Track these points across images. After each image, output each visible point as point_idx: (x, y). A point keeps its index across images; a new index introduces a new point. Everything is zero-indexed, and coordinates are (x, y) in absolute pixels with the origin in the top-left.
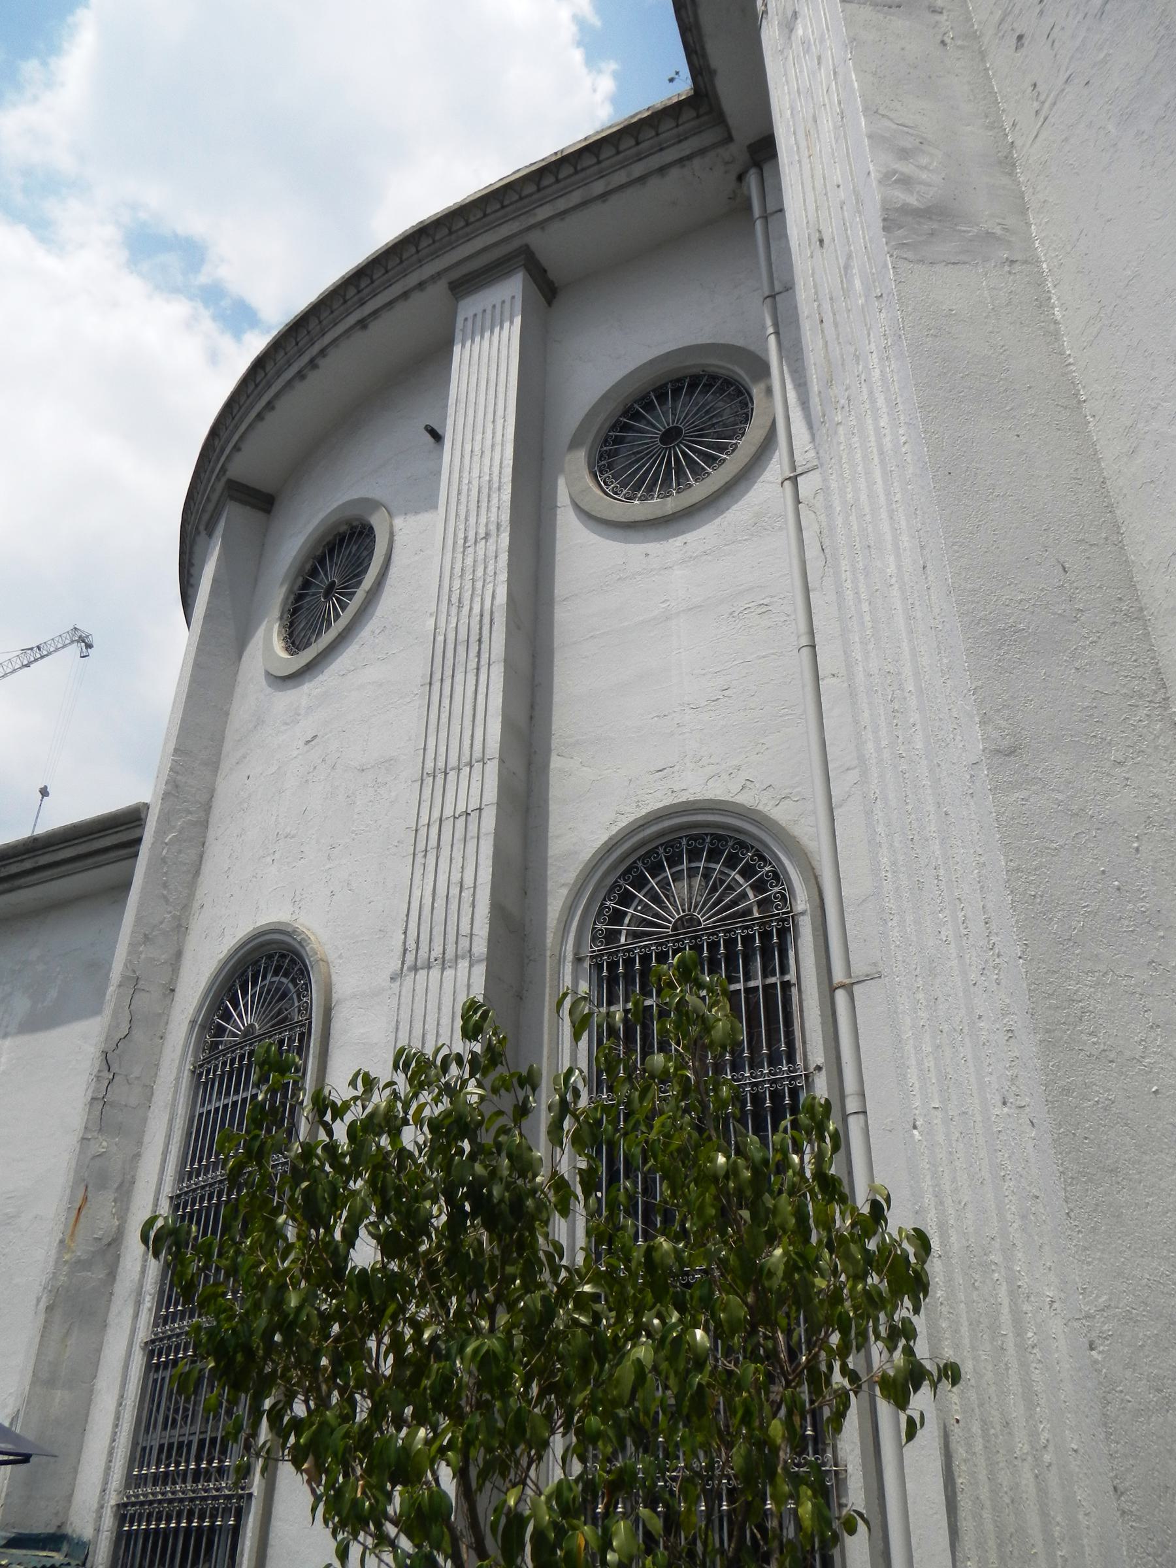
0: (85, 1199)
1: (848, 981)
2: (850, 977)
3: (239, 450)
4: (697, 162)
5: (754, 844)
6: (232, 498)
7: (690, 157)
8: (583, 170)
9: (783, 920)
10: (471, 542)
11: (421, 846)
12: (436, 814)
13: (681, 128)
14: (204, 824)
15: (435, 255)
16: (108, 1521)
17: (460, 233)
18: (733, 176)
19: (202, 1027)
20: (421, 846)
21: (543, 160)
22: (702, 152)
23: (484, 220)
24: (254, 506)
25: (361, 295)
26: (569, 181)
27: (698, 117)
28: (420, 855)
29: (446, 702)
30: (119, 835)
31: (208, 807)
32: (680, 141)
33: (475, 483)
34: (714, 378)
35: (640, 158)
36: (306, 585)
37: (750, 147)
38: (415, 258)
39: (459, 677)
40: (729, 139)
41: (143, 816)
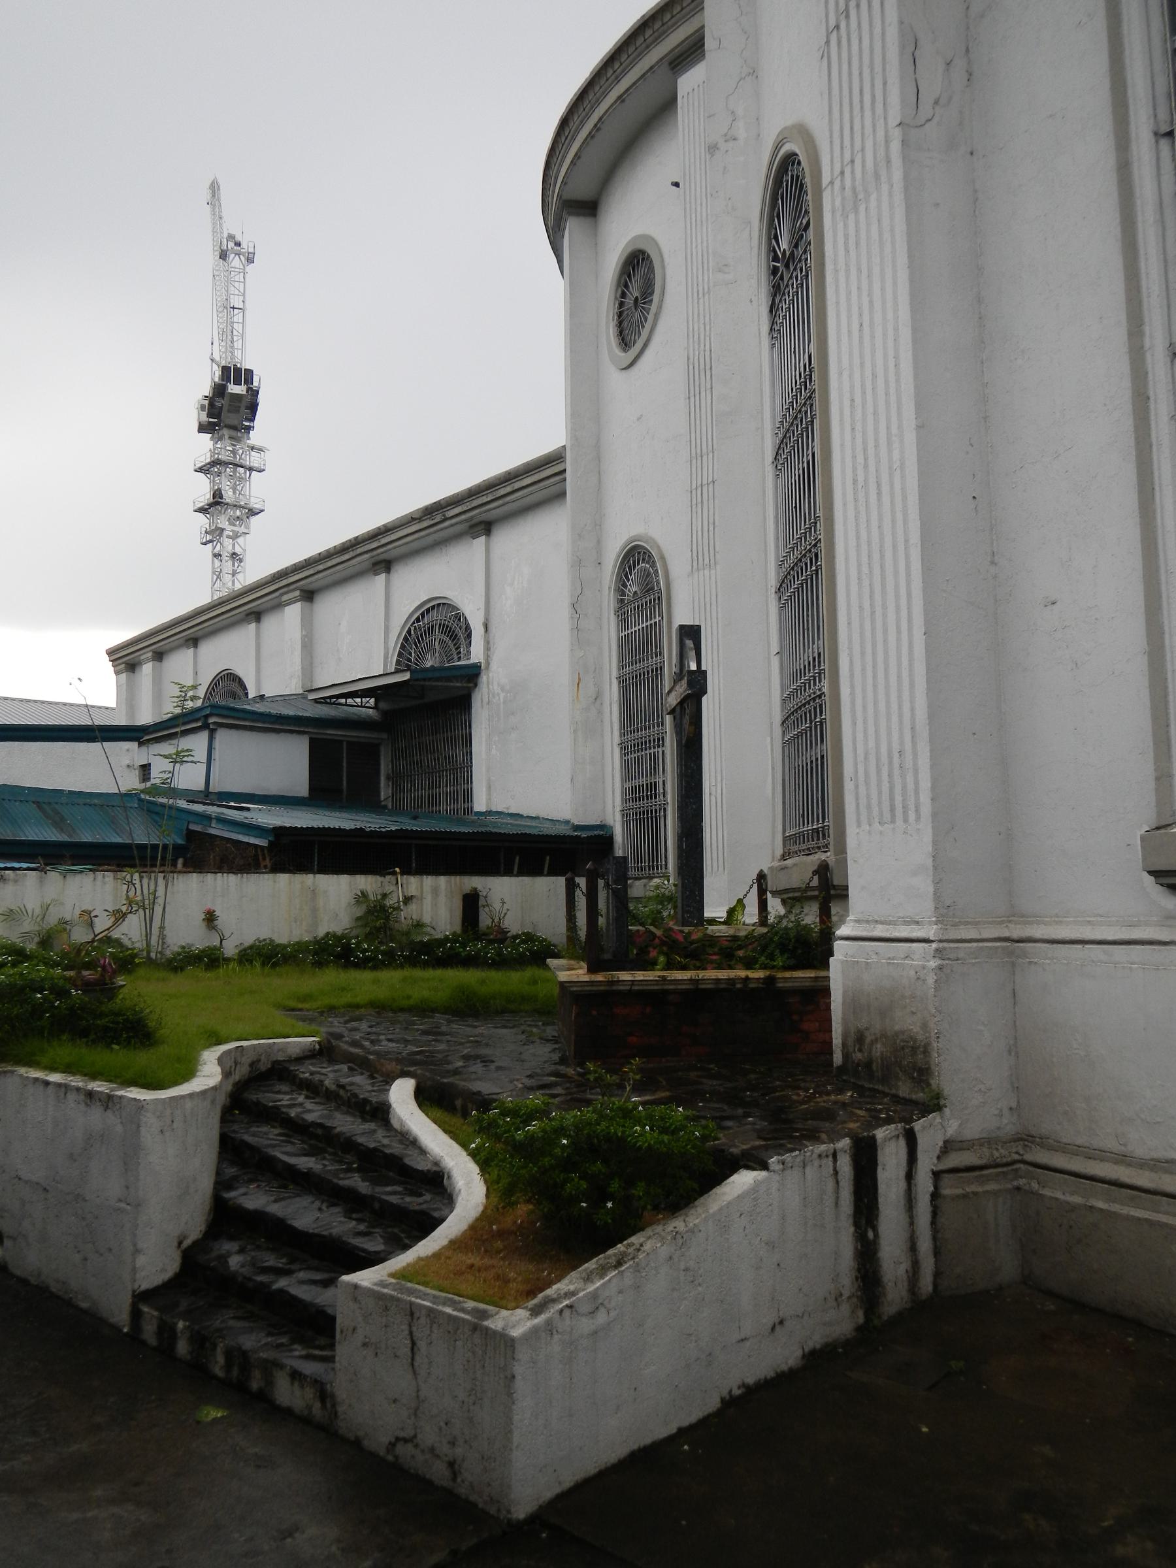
0: (580, 679)
3: (565, 184)
6: (570, 214)
10: (701, 295)
11: (694, 502)
12: (699, 483)
14: (598, 458)
15: (657, 40)
16: (618, 817)
17: (670, 23)
19: (615, 590)
20: (694, 502)
23: (682, 13)
24: (584, 215)
25: (616, 73)
28: (694, 507)
29: (698, 410)
30: (553, 468)
31: (598, 446)
33: (699, 246)
36: (621, 304)
38: (644, 45)
39: (703, 394)
41: (563, 455)
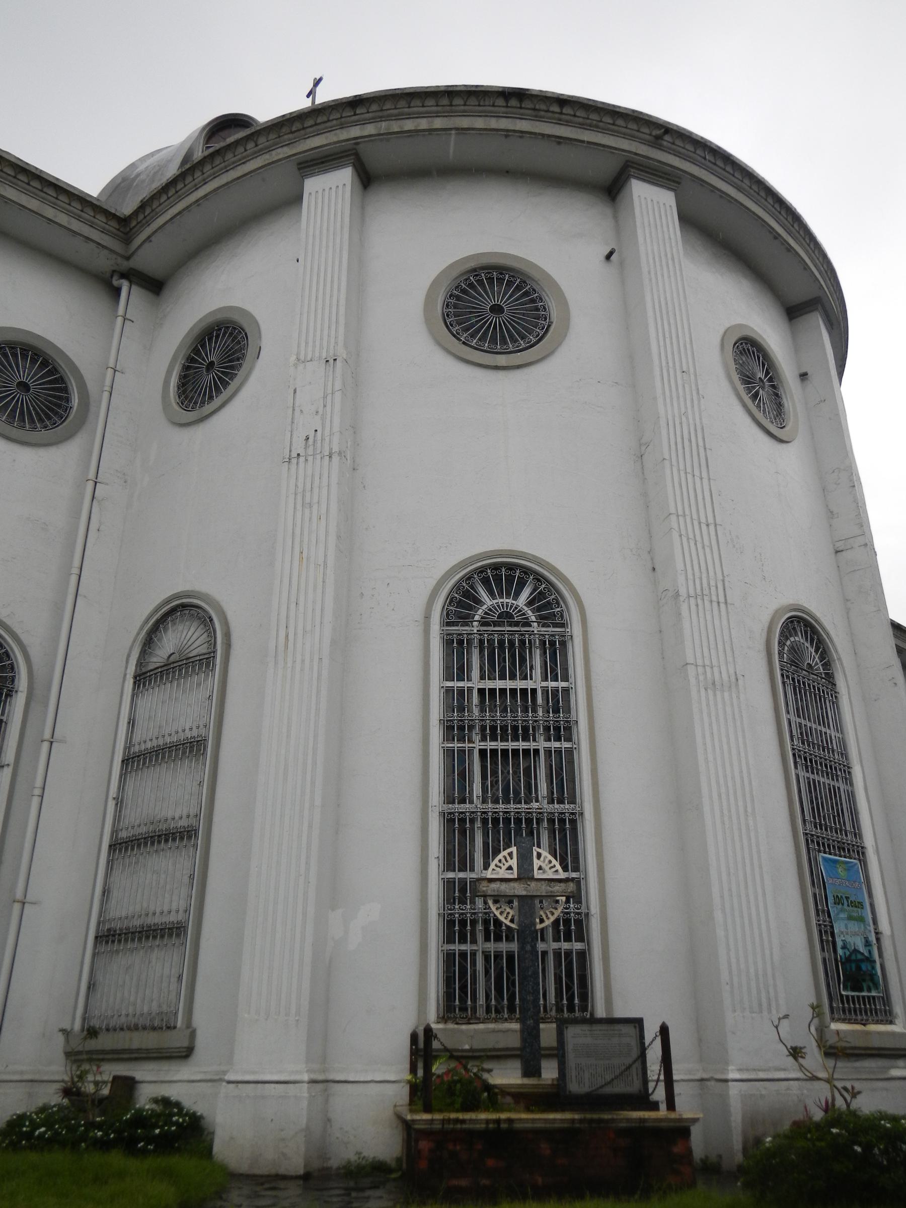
1: (52, 740)
2: (52, 738)
4: (106, 252)
5: (6, 646)
7: (103, 246)
8: (46, 193)
9: (10, 691)
13: (107, 226)
18: (114, 268)
21: (27, 164)
22: (111, 251)
26: (34, 190)
27: (118, 230)
32: (103, 232)
34: (54, 371)
35: (79, 218)
37: (131, 269)
40: (128, 258)
